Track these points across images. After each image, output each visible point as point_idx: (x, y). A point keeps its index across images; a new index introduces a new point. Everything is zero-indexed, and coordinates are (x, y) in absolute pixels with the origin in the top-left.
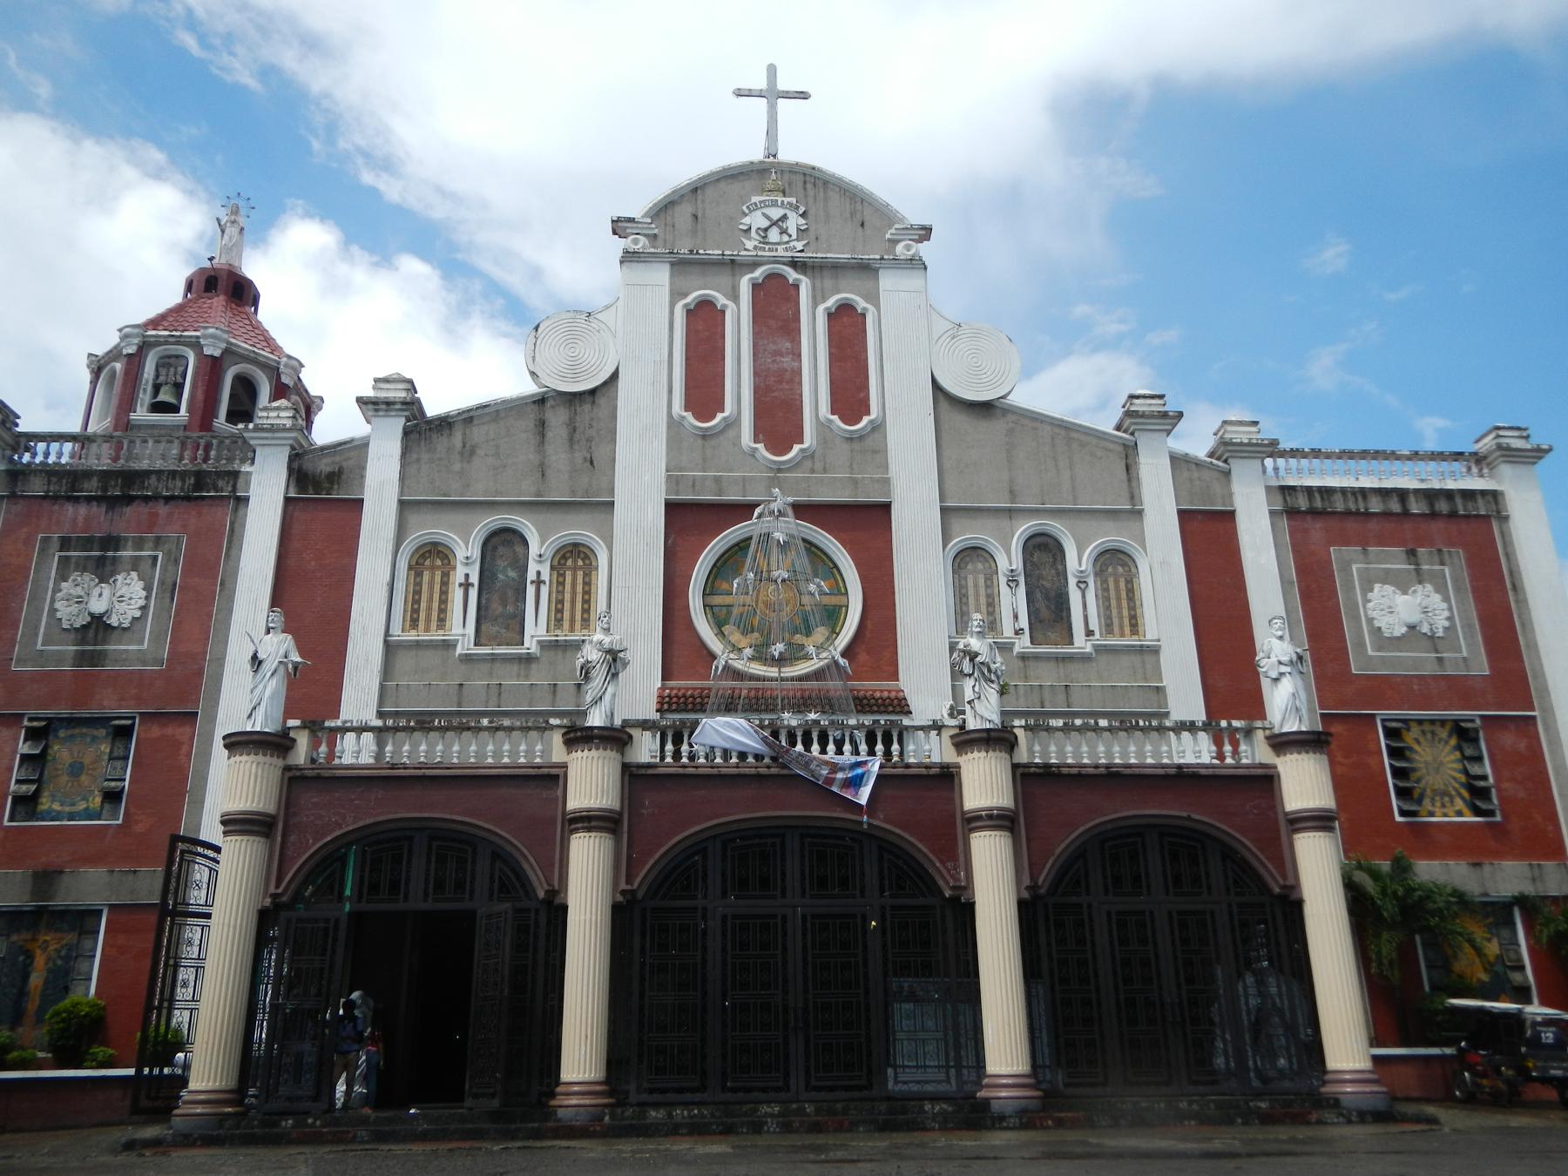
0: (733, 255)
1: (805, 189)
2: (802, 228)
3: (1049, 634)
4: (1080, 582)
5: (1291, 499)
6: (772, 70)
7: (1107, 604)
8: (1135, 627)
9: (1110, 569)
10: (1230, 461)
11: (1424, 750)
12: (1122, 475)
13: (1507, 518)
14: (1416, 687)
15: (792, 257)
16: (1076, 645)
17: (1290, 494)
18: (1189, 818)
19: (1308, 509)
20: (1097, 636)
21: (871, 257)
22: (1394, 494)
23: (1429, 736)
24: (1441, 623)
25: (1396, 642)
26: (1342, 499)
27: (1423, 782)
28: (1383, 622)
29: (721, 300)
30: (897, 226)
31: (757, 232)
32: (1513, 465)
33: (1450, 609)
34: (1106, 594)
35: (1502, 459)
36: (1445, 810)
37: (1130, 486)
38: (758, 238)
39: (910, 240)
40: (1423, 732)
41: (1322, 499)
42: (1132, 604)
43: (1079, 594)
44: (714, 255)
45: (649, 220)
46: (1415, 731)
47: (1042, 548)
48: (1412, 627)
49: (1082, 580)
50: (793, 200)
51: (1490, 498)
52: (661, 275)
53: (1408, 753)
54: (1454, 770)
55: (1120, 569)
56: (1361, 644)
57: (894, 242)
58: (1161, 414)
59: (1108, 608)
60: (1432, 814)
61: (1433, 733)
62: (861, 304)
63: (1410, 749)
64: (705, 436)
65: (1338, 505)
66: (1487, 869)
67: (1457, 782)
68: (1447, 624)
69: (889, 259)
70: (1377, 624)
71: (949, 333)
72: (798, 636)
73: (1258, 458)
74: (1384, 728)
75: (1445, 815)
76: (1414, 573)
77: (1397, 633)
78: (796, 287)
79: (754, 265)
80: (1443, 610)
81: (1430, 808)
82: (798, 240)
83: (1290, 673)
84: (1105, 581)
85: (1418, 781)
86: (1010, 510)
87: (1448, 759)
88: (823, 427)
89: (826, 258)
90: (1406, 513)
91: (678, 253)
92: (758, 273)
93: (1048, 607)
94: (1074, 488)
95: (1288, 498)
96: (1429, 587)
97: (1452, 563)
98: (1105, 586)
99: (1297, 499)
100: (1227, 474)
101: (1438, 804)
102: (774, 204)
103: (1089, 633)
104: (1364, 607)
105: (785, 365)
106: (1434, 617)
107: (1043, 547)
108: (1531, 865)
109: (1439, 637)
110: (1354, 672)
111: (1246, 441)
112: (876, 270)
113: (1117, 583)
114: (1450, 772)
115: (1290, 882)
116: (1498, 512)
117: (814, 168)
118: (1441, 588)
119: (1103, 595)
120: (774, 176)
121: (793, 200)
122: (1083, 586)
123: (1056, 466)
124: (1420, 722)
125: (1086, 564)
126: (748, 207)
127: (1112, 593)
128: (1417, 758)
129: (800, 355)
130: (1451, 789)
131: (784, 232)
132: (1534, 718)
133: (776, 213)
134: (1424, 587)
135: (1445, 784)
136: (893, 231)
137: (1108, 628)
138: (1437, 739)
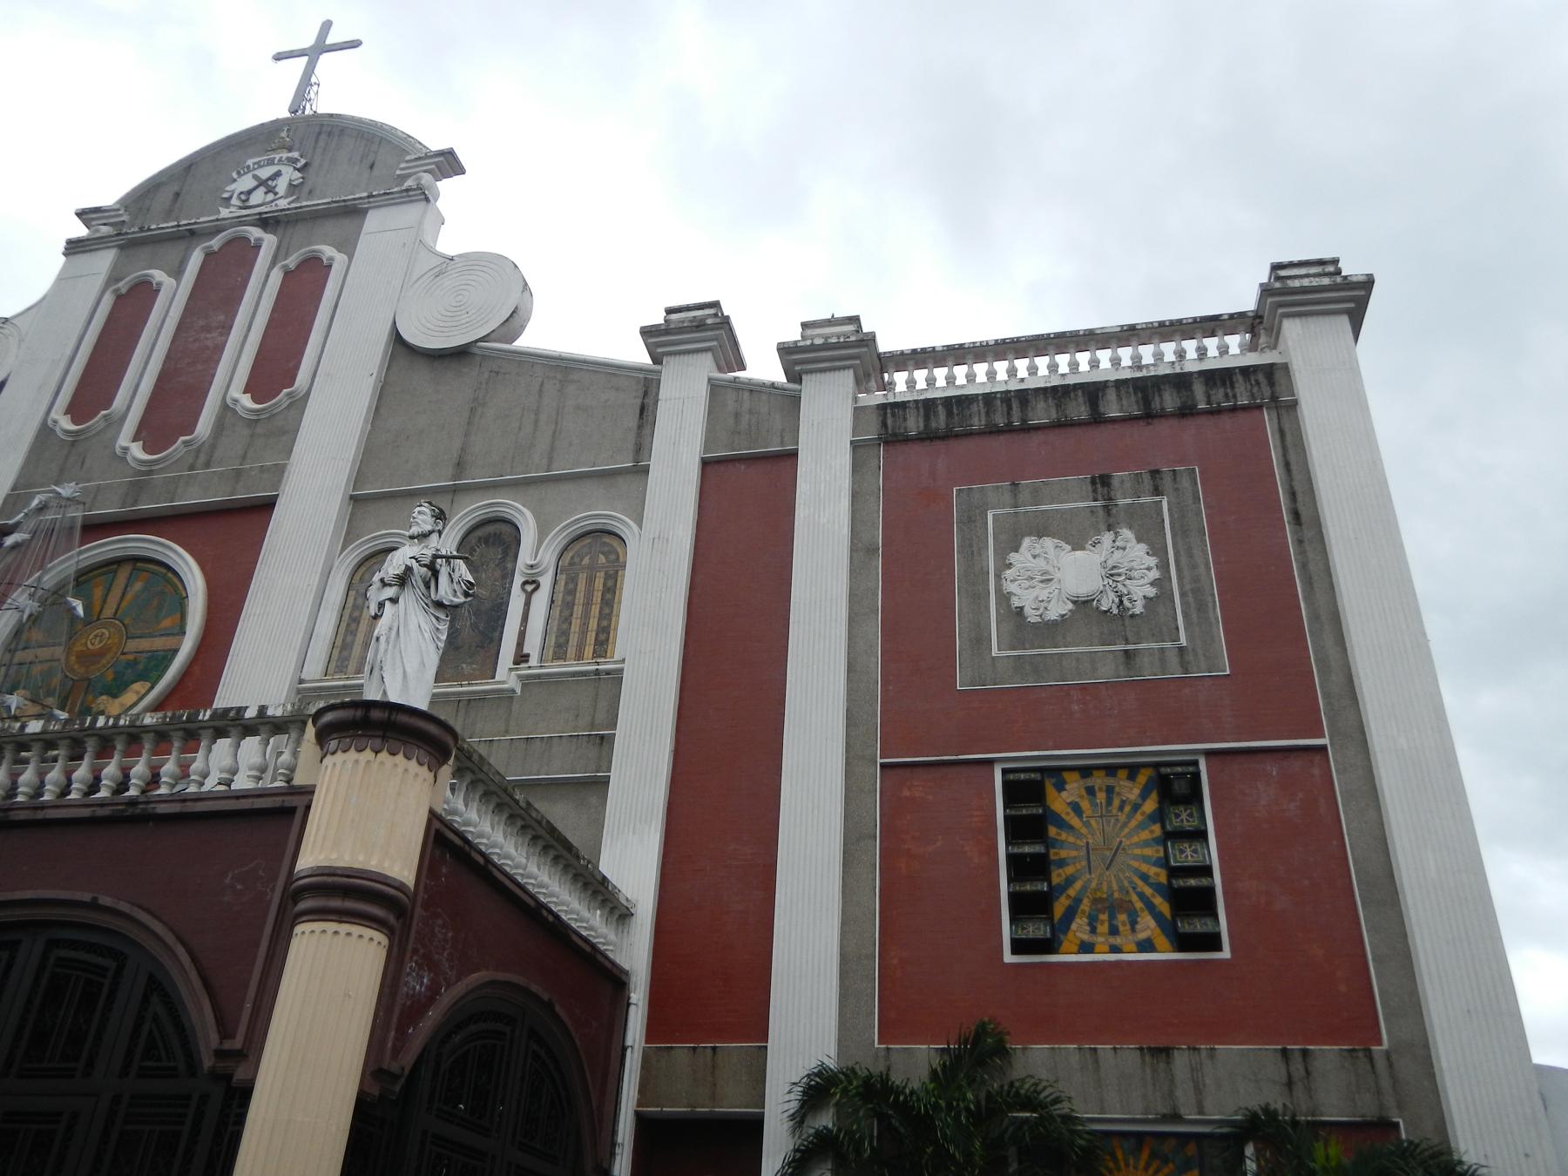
0: (190, 224)
1: (317, 141)
2: (294, 183)
3: (464, 666)
4: (526, 583)
5: (895, 421)
6: (327, 26)
7: (567, 613)
8: (603, 643)
9: (586, 561)
10: (804, 377)
11: (1087, 825)
12: (631, 421)
13: (1294, 405)
14: (1076, 707)
15: (260, 214)
16: (497, 678)
17: (893, 415)
18: (94, 905)
19: (920, 433)
20: (533, 661)
21: (357, 196)
22: (1080, 393)
23: (1101, 797)
24: (1140, 590)
25: (1051, 630)
26: (983, 411)
27: (1078, 885)
28: (1026, 597)
29: (158, 275)
30: (408, 158)
31: (239, 198)
32: (1304, 319)
33: (1163, 566)
34: (569, 598)
35: (1280, 311)
36: (1118, 941)
37: (639, 435)
38: (239, 203)
39: (425, 172)
40: (1091, 791)
41: (950, 414)
42: (607, 611)
43: (523, 597)
44: (168, 228)
45: (116, 207)
46: (1074, 788)
47: (491, 540)
48: (1083, 605)
49: (530, 580)
50: (295, 154)
51: (1261, 377)
52: (104, 260)
53: (1052, 831)
54: (1145, 859)
55: (602, 559)
56: (979, 640)
57: (404, 178)
58: (694, 324)
59: (567, 620)
60: (1086, 948)
61: (1110, 790)
62: (328, 251)
63: (1062, 824)
64: (75, 440)
65: (975, 421)
66: (1181, 1061)
67: (1150, 885)
68: (1151, 592)
69: (379, 195)
70: (1016, 602)
71: (438, 269)
72: (104, 697)
73: (848, 367)
74: (1006, 784)
75: (1115, 949)
76: (1101, 512)
77: (1052, 615)
78: (258, 247)
79: (219, 230)
80: (1149, 569)
81: (1085, 937)
82: (286, 198)
83: (391, 600)
84: (573, 580)
85: (1070, 881)
86: (455, 490)
87: (1135, 839)
88: (226, 409)
89: (301, 207)
90: (1097, 420)
91: (127, 233)
92: (215, 243)
93: (474, 626)
94: (552, 448)
95: (889, 422)
96: (1127, 534)
97: (1177, 490)
98: (571, 586)
99: (905, 419)
100: (794, 401)
101: (1103, 928)
102: (271, 162)
103: (521, 658)
104: (998, 577)
105: (209, 343)
106: (1128, 582)
107: (486, 540)
108: (1284, 1052)
109: (1132, 616)
110: (958, 688)
111: (819, 341)
112: (363, 212)
113: (591, 581)
114: (1135, 864)
115: (237, 1043)
116: (1274, 398)
117: (331, 115)
118: (1150, 535)
119: (563, 601)
120: (284, 134)
121: (295, 154)
122: (529, 588)
123: (536, 422)
124: (1086, 771)
125: (548, 557)
126: (239, 173)
127: (580, 596)
128: (1071, 839)
129: (231, 327)
130: (1135, 898)
131: (271, 190)
132: (1323, 748)
133: (265, 173)
134: (1116, 534)
135: (1122, 889)
136: (403, 165)
137: (560, 653)
138: (1116, 802)
